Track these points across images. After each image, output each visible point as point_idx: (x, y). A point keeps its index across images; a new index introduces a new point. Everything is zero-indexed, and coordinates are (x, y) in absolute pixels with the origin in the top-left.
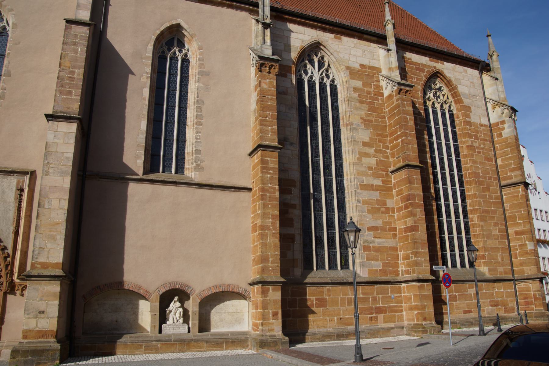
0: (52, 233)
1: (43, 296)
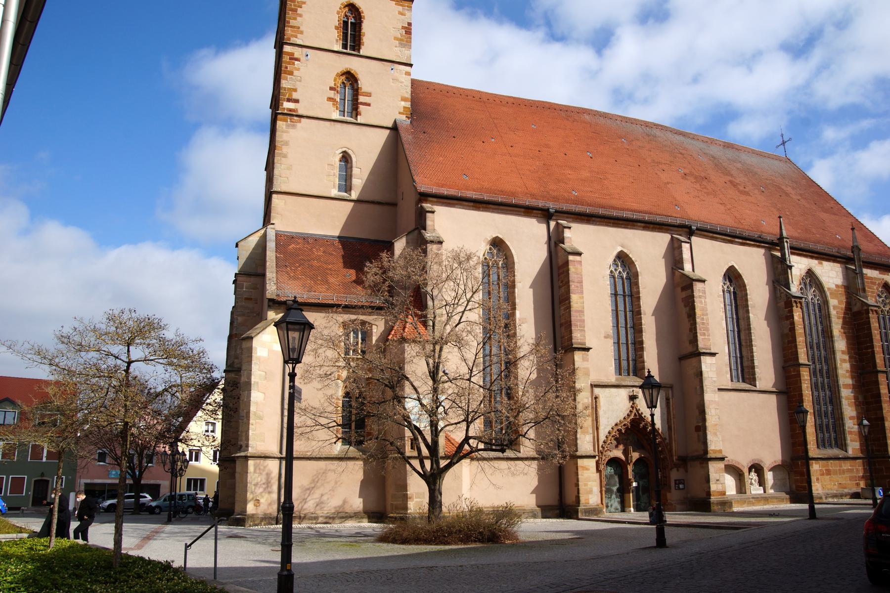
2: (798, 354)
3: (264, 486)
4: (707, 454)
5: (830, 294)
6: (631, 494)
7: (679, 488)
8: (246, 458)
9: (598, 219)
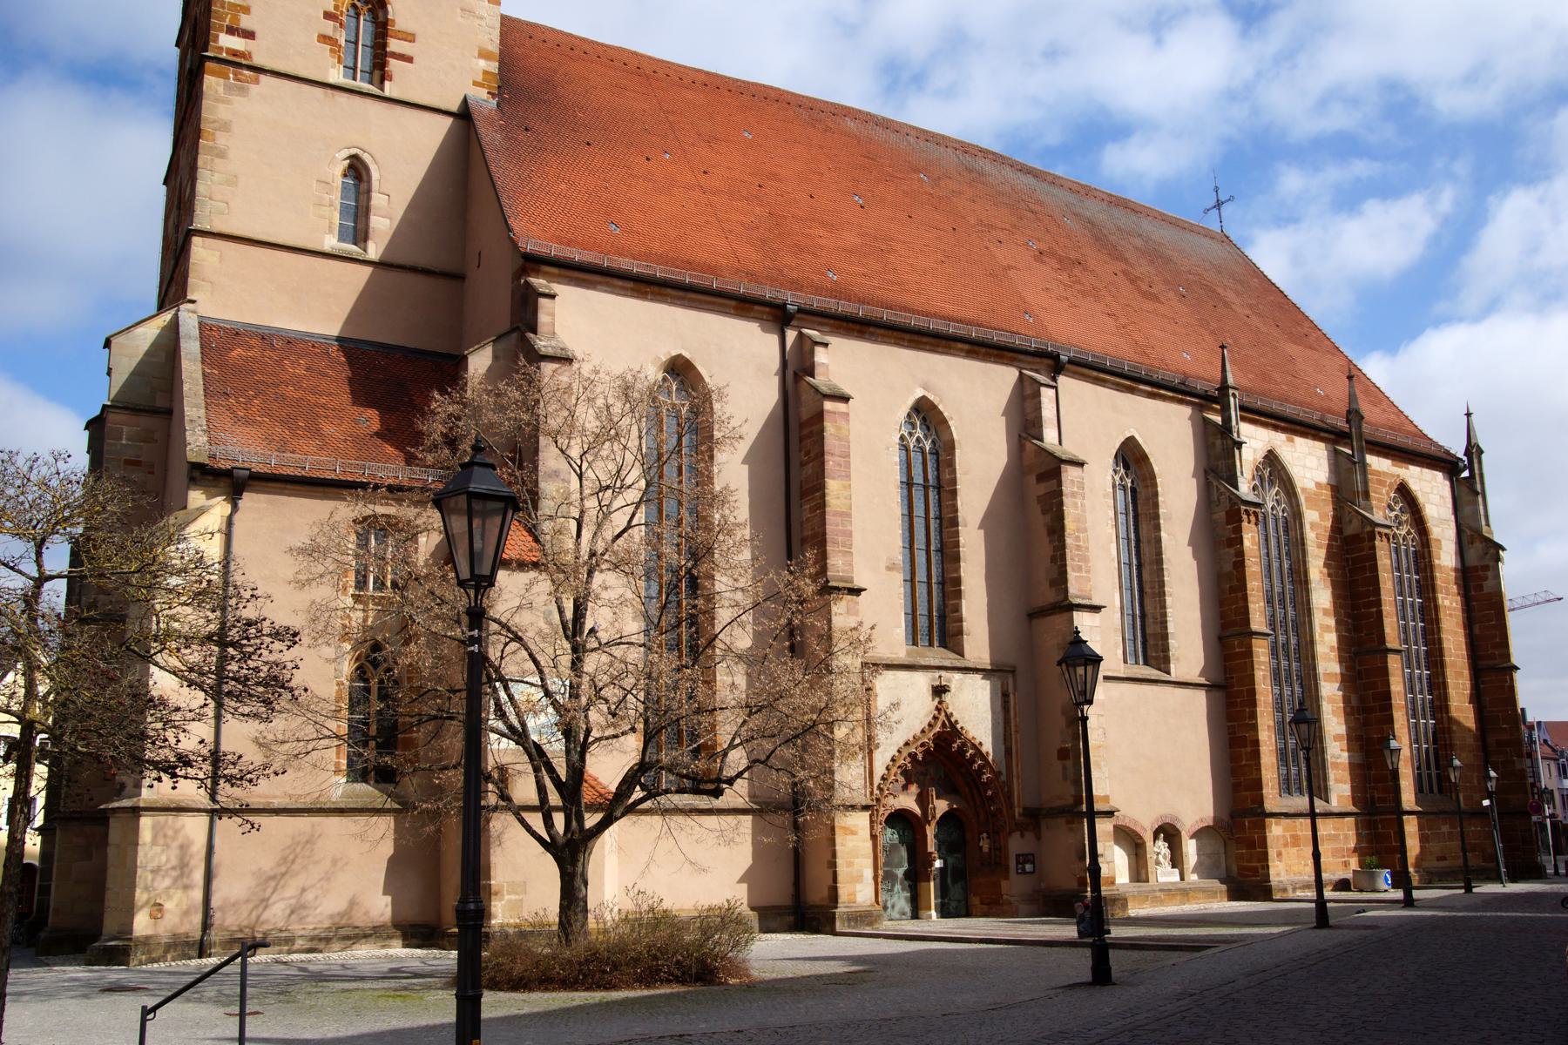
2: (1248, 613)
3: (174, 873)
5: (1307, 499)
6: (932, 884)
7: (1024, 872)
8: (136, 812)
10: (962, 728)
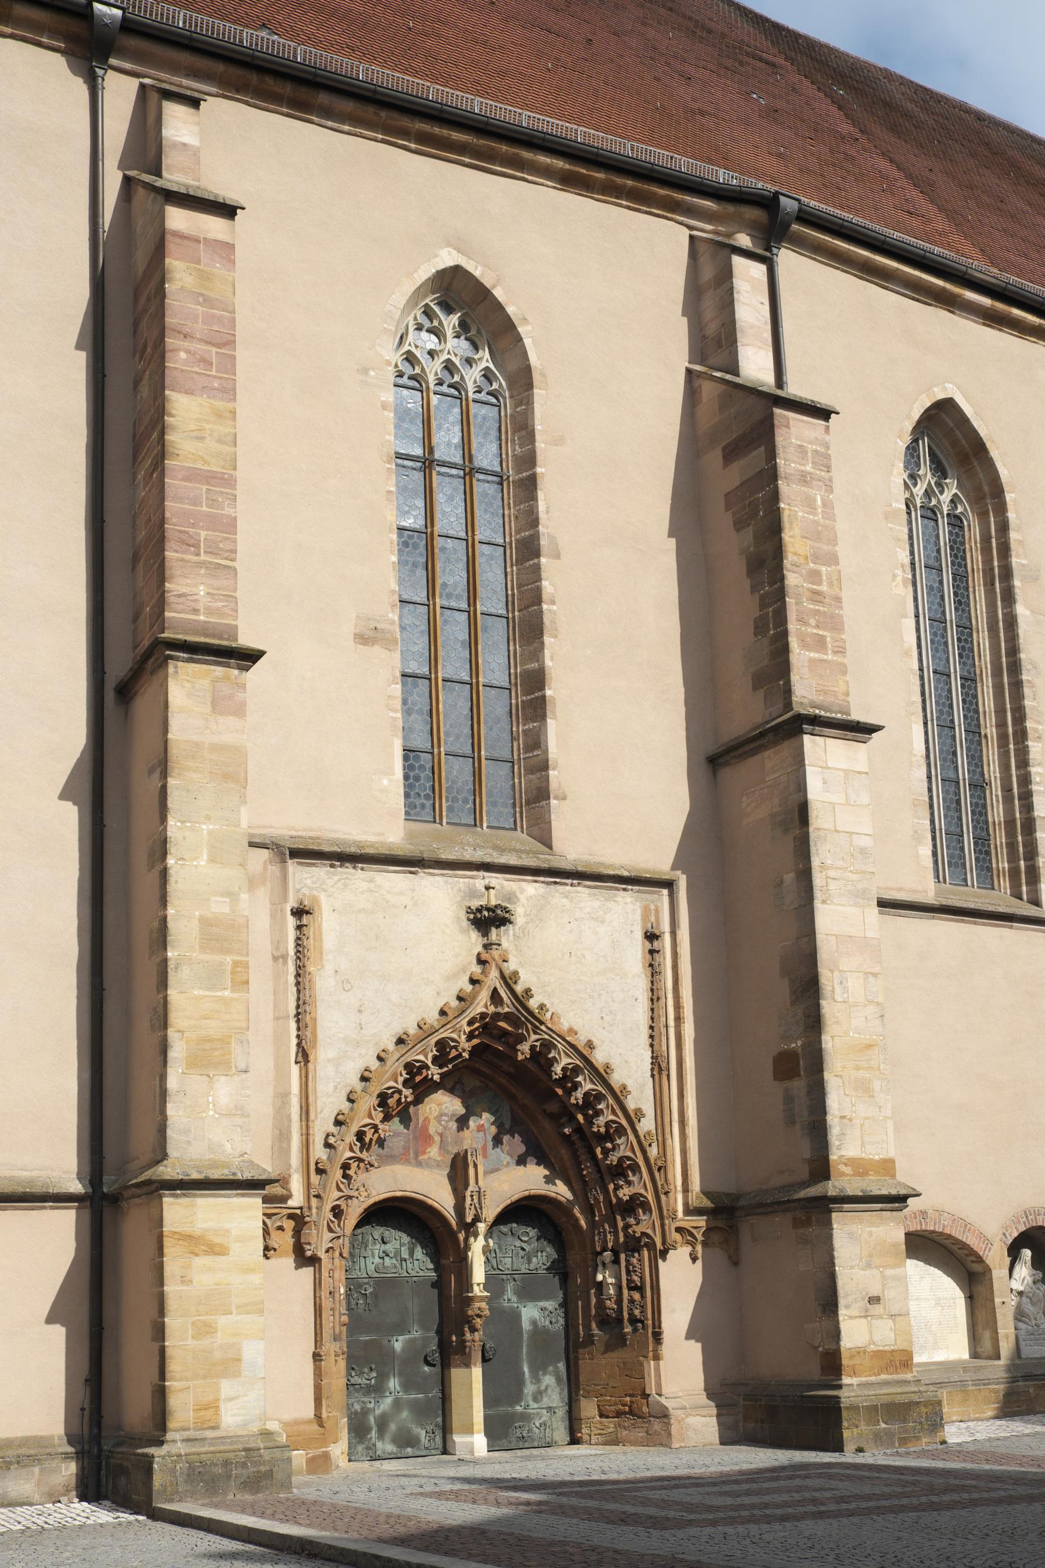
0: (861, 1074)
1: (870, 1256)
4: (827, 1177)
9: (348, 106)
10: (542, 1007)
